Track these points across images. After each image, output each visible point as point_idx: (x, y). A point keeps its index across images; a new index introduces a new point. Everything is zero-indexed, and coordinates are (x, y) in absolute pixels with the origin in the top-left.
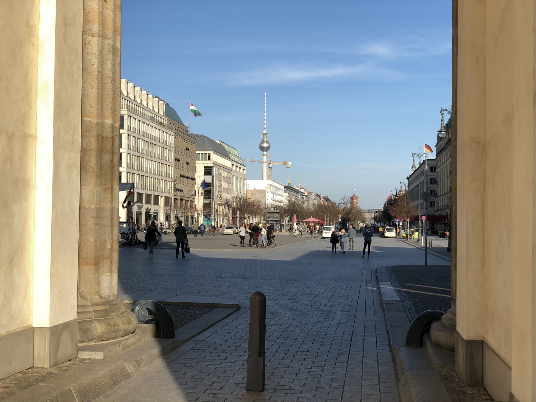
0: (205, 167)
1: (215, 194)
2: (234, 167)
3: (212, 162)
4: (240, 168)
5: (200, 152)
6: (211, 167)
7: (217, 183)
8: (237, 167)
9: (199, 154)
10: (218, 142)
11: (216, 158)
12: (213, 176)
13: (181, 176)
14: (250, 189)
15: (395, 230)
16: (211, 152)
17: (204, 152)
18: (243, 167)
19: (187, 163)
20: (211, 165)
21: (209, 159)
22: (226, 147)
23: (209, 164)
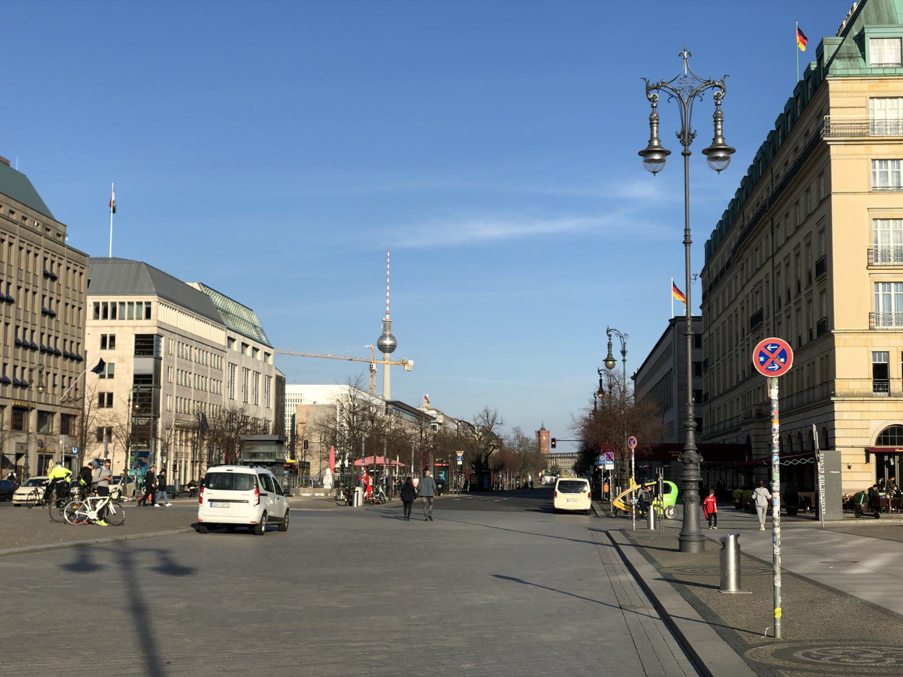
0: (137, 336)
1: (168, 403)
2: (236, 346)
3: (155, 323)
4: (255, 350)
5: (126, 299)
6: (151, 336)
7: (169, 377)
8: (245, 345)
9: (122, 304)
10: (196, 286)
11: (166, 315)
12: (158, 359)
13: (18, 344)
14: (304, 403)
15: (588, 489)
16: (153, 299)
17: (135, 299)
18: (263, 349)
19: (48, 314)
20: (153, 331)
21: (148, 316)
22: (217, 300)
23: (147, 327)
